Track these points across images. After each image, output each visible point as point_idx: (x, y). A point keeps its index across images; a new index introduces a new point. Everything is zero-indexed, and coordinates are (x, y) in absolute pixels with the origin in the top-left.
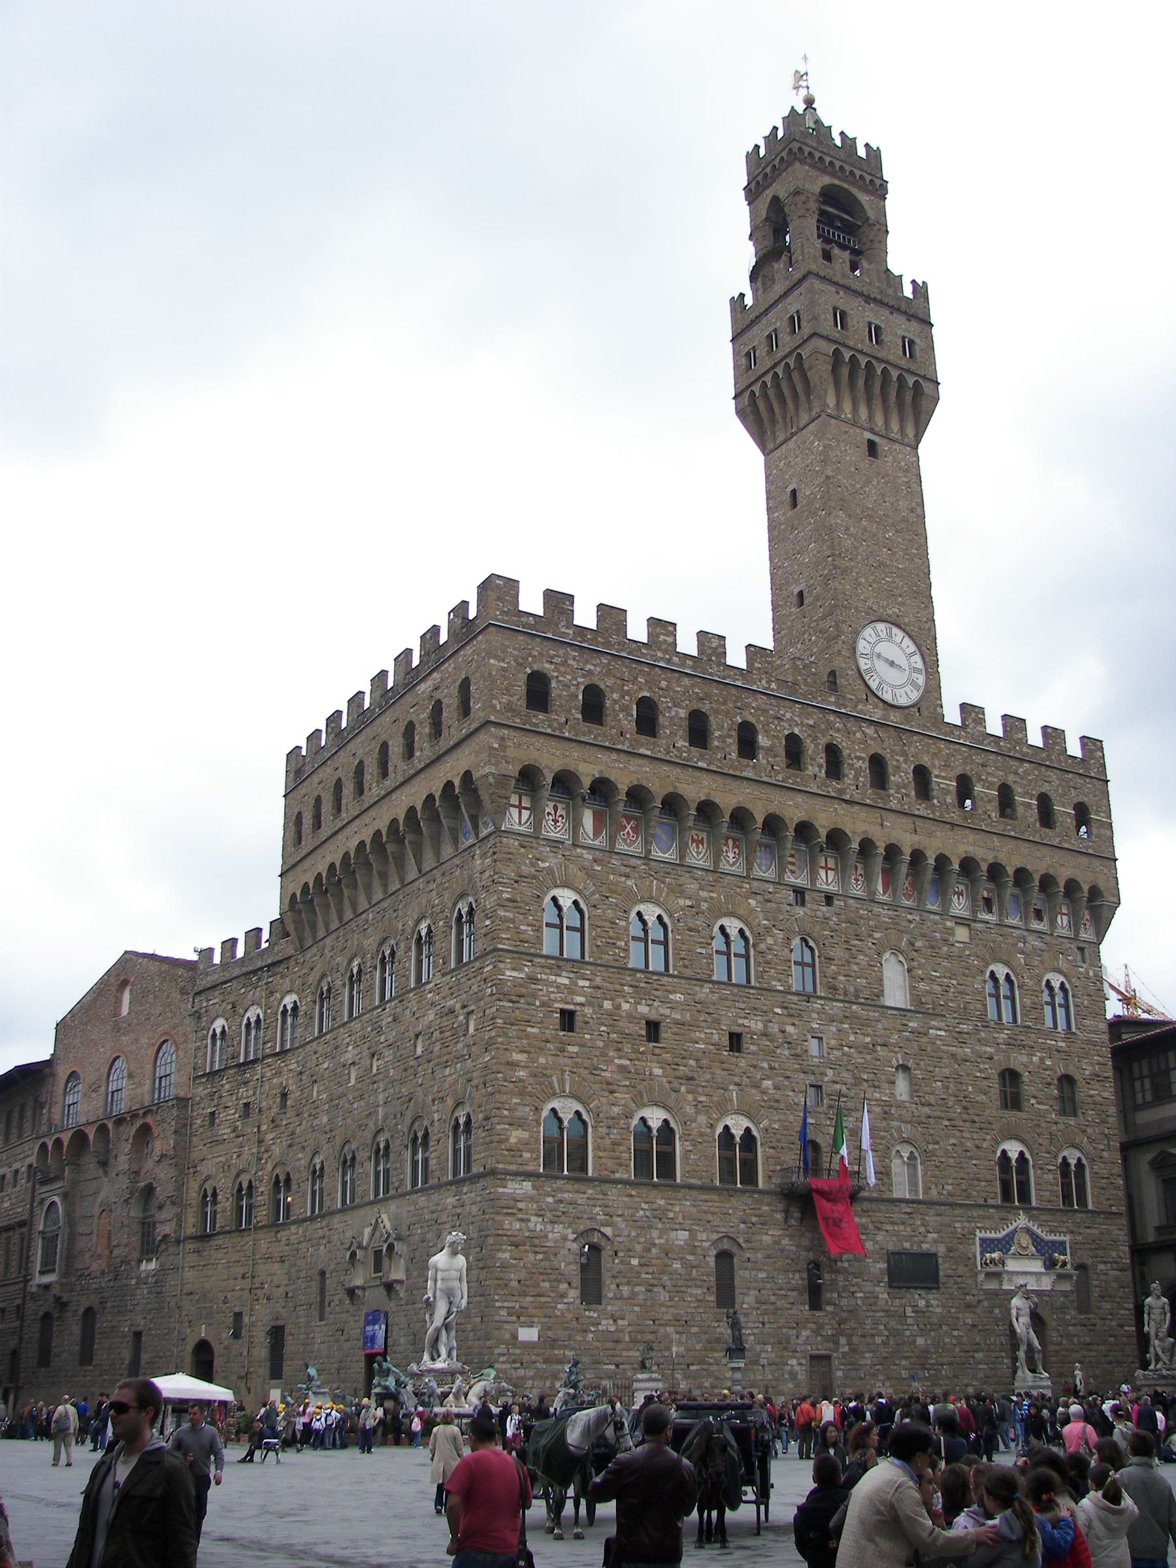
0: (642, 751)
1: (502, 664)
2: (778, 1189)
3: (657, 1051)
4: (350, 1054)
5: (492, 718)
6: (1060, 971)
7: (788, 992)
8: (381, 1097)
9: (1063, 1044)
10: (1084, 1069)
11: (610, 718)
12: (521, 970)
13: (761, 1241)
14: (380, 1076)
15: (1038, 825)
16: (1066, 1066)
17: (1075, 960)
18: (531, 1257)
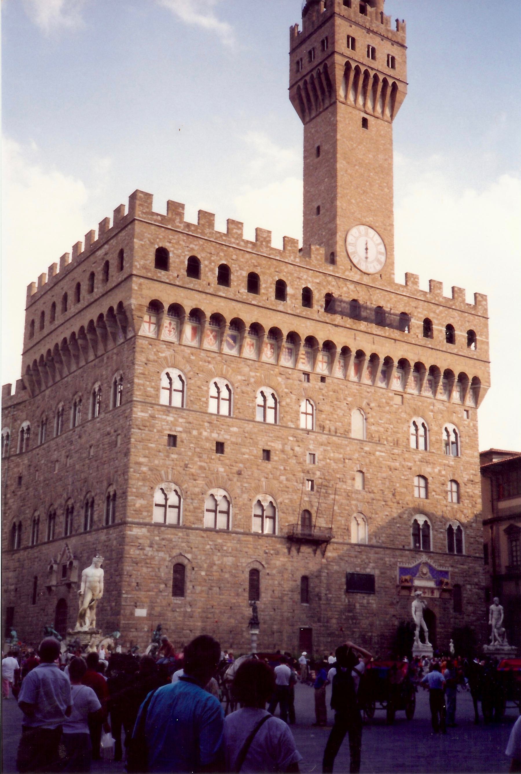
0: (221, 294)
1: (141, 242)
2: (286, 536)
3: (222, 458)
4: (55, 456)
5: (134, 272)
7: (297, 428)
8: (70, 480)
10: (464, 477)
11: (202, 276)
12: (147, 412)
13: (275, 564)
14: (71, 468)
16: (454, 474)
17: (462, 417)
18: (145, 570)
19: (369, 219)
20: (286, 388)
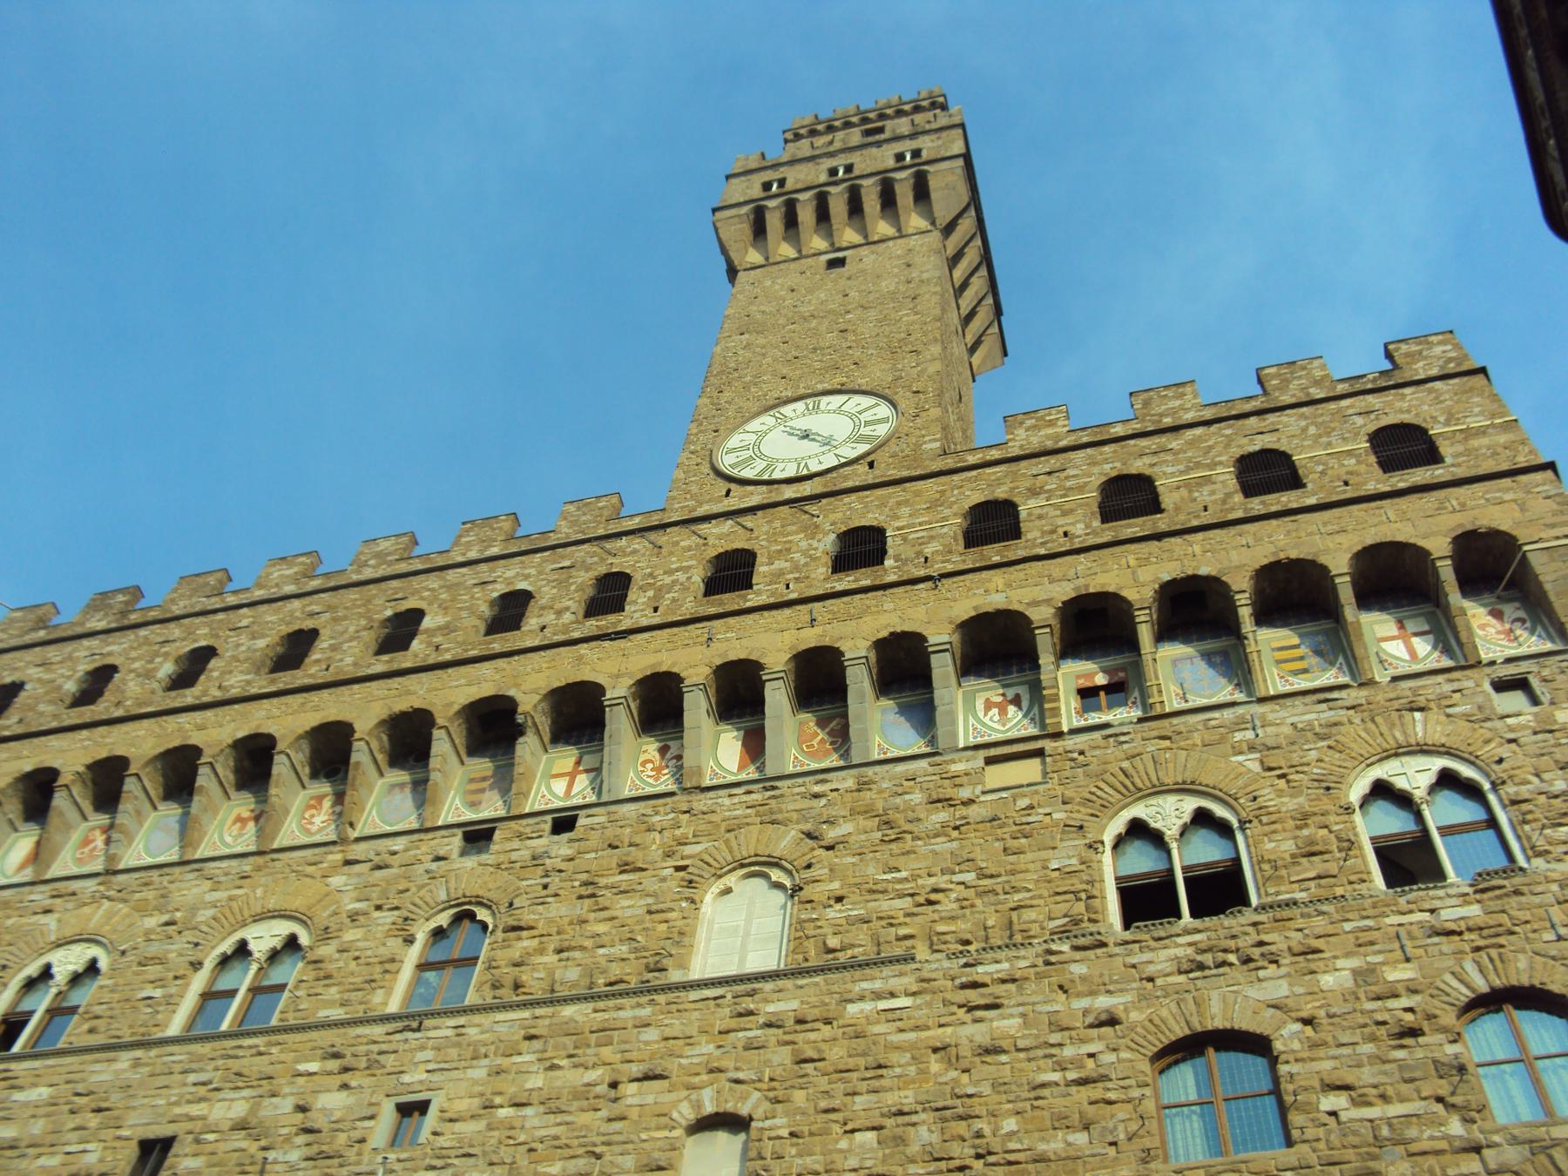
6: (1424, 750)
9: (1474, 910)
19: (835, 383)
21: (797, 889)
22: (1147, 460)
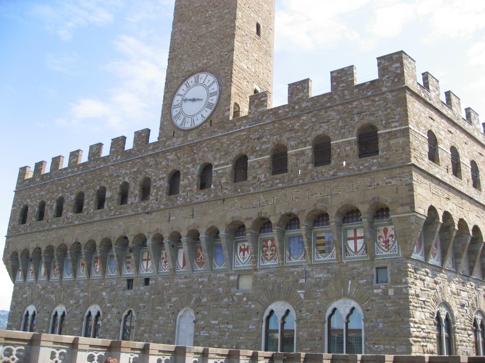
6: (349, 297)
15: (310, 167)
20: (109, 302)
21: (195, 322)
22: (287, 135)
